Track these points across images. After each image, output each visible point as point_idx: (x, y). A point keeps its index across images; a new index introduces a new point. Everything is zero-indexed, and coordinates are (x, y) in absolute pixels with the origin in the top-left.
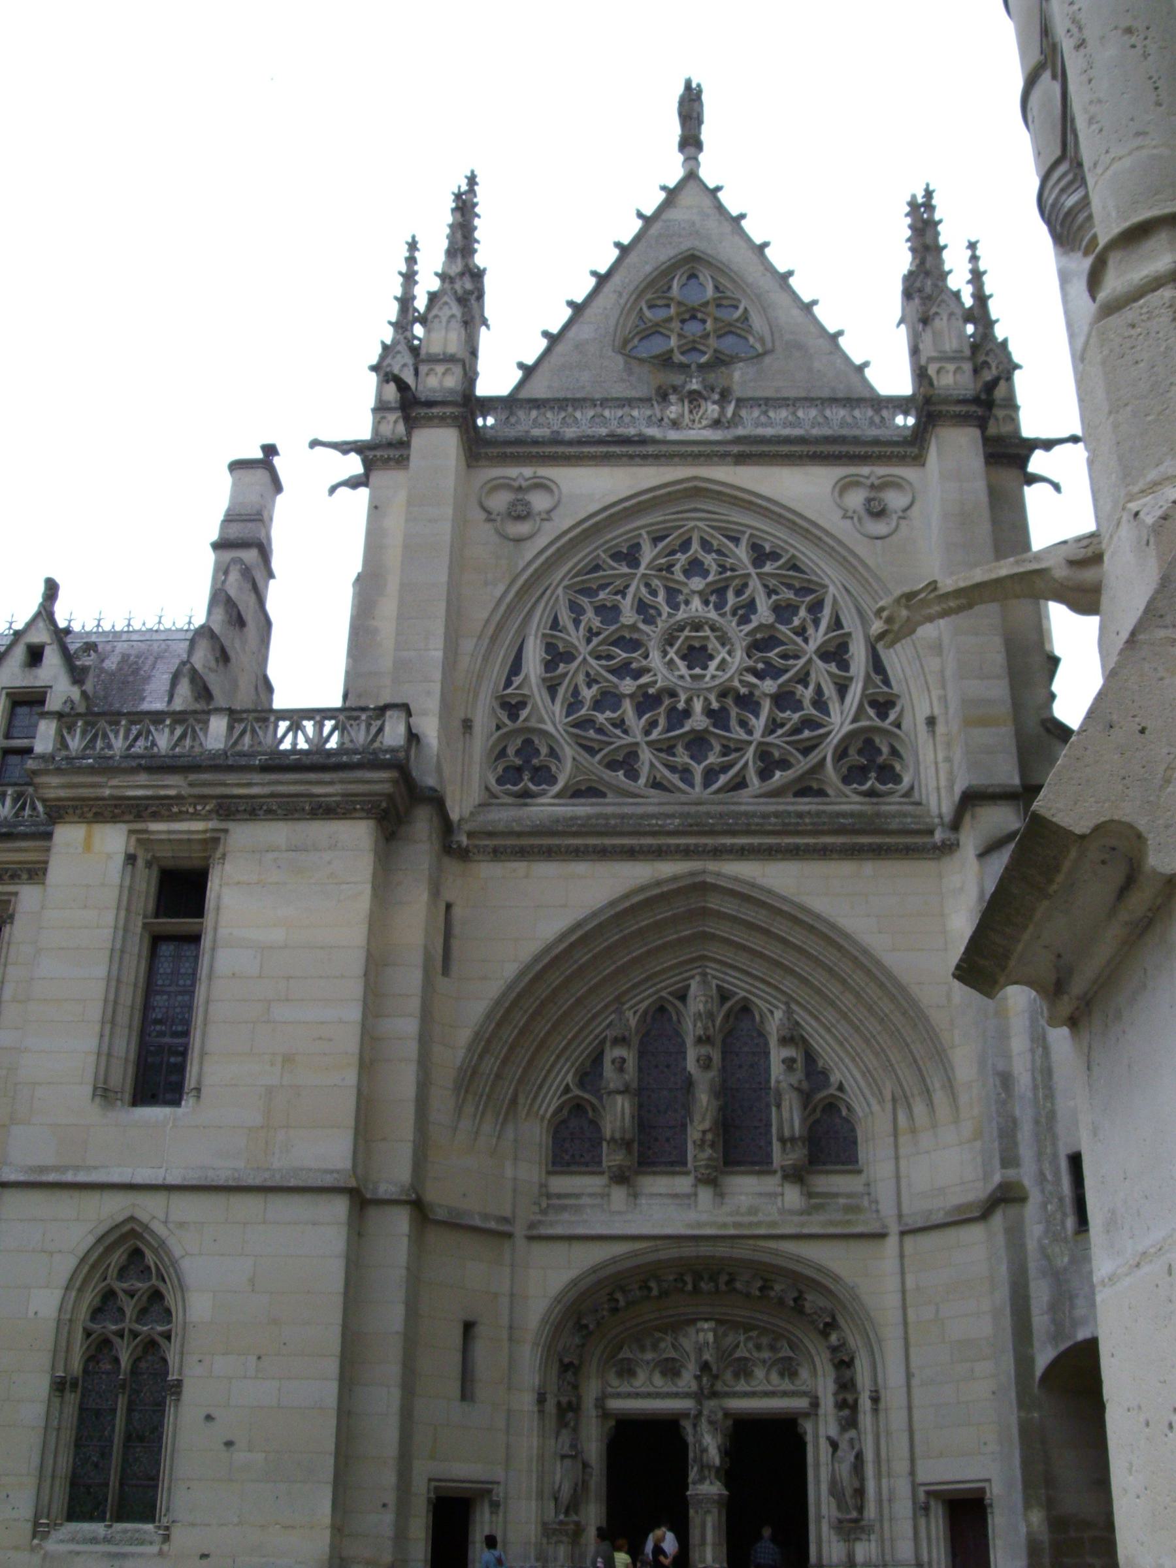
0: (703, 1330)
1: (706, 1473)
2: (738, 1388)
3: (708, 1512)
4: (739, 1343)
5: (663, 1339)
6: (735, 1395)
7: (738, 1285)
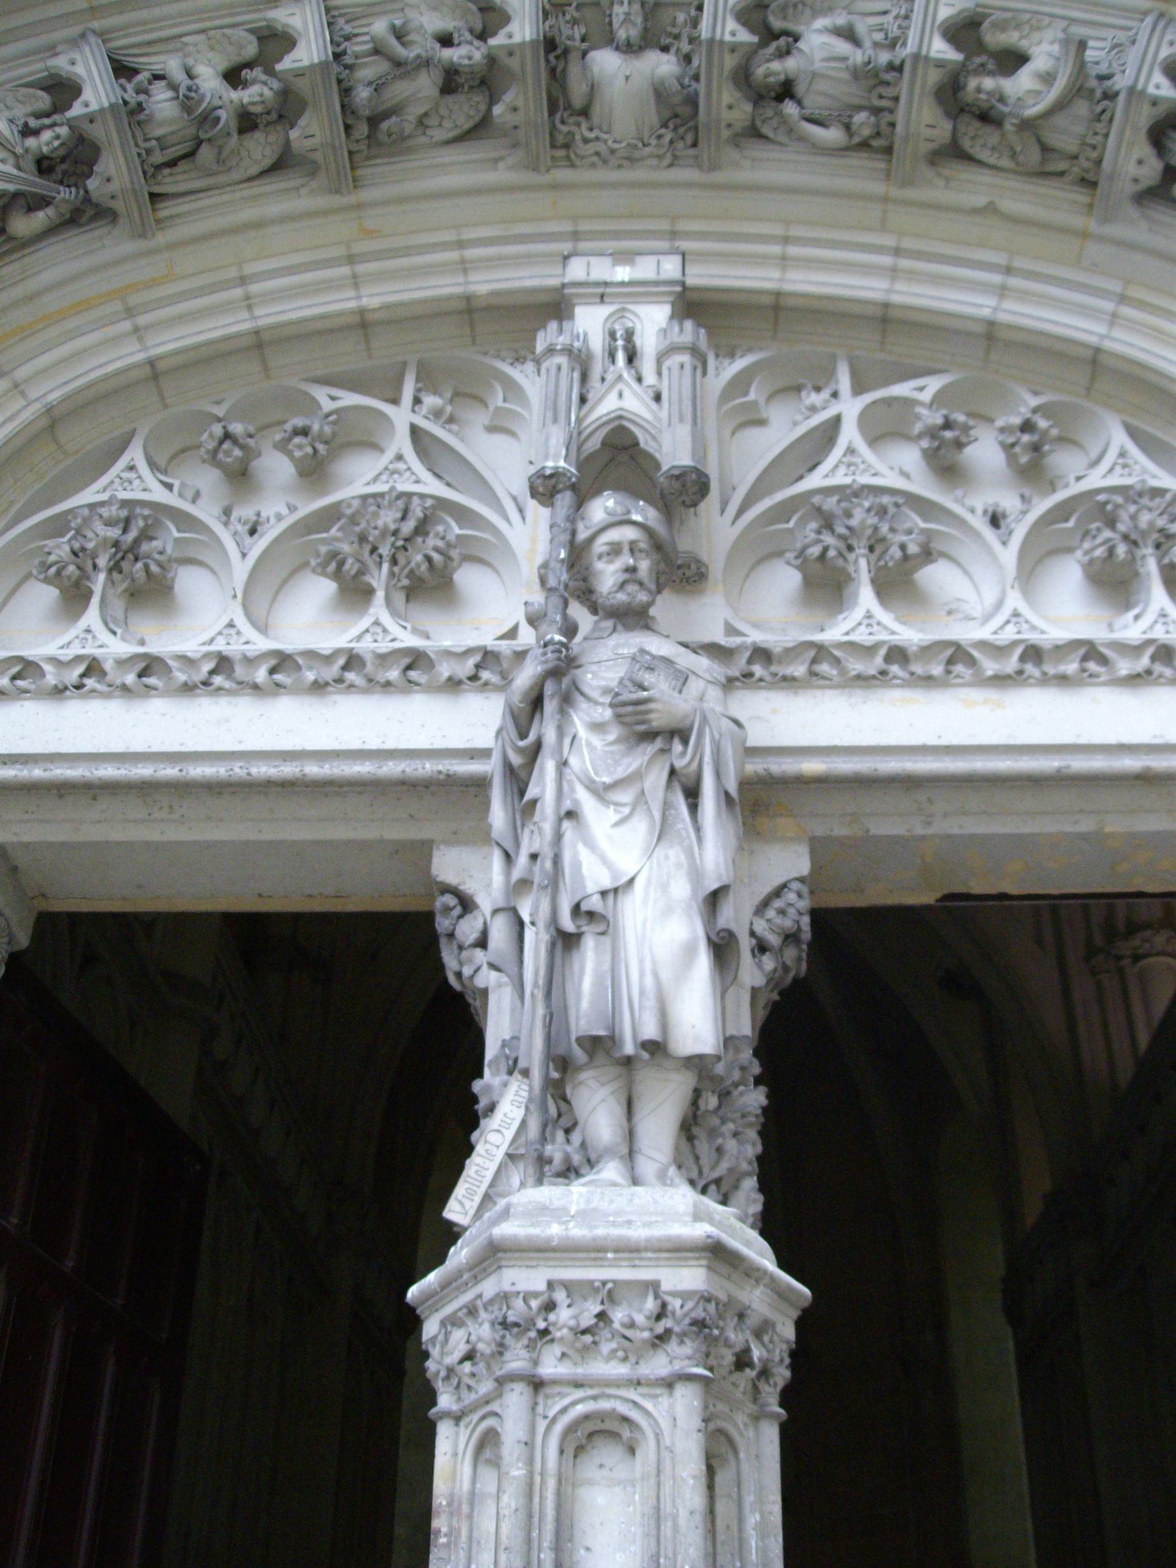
0: (602, 292)
1: (598, 1108)
2: (834, 633)
3: (596, 1434)
4: (837, 421)
5: (357, 435)
6: (820, 667)
7: (818, 43)
